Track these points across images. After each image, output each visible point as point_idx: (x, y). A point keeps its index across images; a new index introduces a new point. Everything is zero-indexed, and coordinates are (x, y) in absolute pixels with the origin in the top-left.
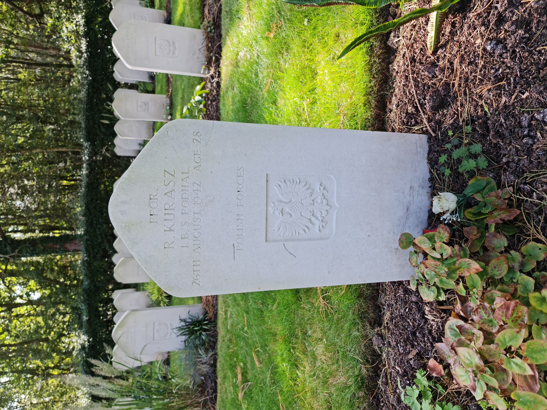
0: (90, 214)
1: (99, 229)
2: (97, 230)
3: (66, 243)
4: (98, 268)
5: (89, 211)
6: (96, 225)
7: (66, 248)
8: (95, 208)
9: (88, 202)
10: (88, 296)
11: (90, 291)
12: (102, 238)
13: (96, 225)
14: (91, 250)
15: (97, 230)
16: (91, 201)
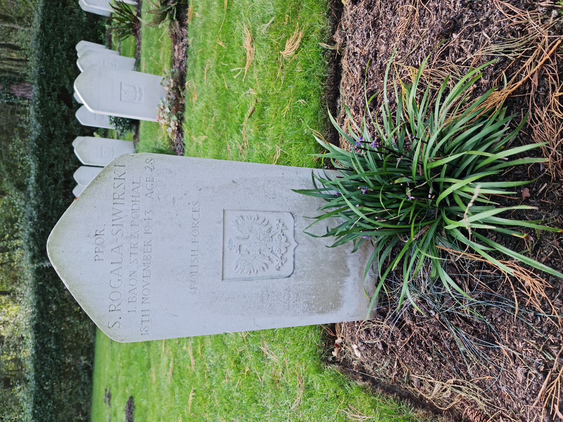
0: (47, 35)
1: (58, 58)
2: (55, 59)
3: (13, 84)
4: (55, 111)
5: (45, 32)
6: (54, 53)
7: (12, 90)
8: (53, 28)
9: (43, 22)
10: (40, 146)
11: (42, 140)
12: (60, 71)
13: (54, 53)
14: (45, 84)
15: (55, 59)
16: (49, 20)
